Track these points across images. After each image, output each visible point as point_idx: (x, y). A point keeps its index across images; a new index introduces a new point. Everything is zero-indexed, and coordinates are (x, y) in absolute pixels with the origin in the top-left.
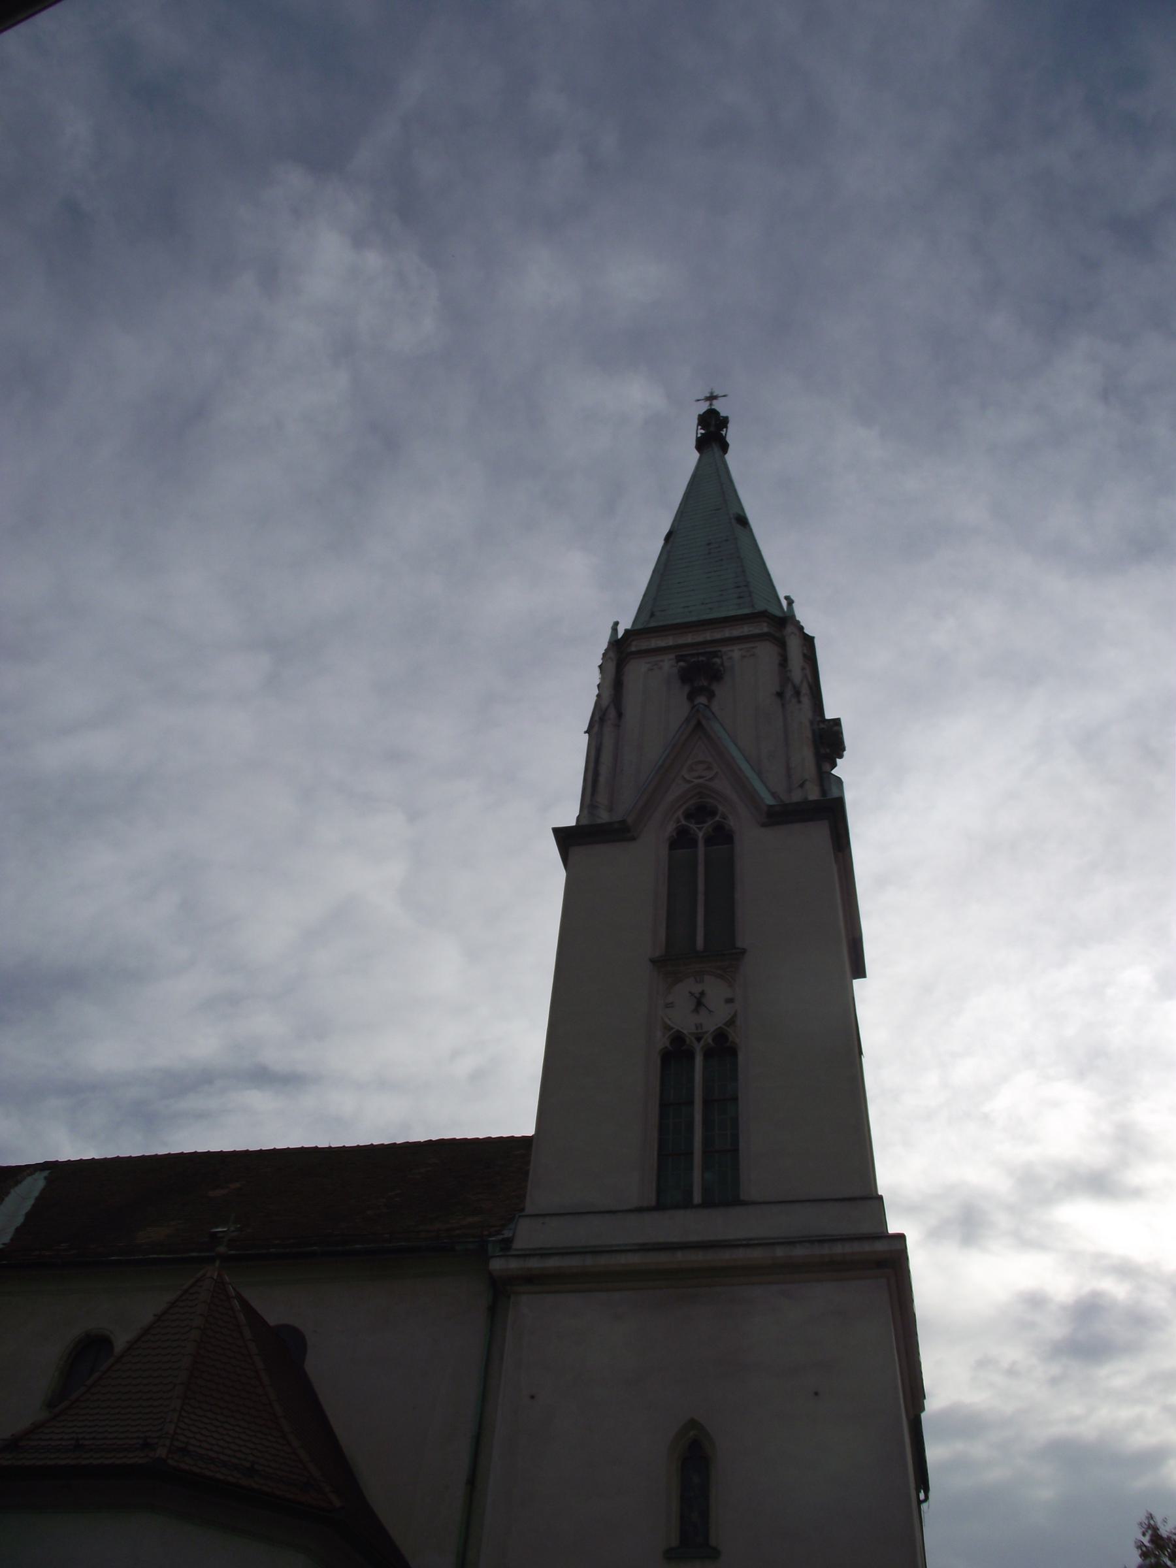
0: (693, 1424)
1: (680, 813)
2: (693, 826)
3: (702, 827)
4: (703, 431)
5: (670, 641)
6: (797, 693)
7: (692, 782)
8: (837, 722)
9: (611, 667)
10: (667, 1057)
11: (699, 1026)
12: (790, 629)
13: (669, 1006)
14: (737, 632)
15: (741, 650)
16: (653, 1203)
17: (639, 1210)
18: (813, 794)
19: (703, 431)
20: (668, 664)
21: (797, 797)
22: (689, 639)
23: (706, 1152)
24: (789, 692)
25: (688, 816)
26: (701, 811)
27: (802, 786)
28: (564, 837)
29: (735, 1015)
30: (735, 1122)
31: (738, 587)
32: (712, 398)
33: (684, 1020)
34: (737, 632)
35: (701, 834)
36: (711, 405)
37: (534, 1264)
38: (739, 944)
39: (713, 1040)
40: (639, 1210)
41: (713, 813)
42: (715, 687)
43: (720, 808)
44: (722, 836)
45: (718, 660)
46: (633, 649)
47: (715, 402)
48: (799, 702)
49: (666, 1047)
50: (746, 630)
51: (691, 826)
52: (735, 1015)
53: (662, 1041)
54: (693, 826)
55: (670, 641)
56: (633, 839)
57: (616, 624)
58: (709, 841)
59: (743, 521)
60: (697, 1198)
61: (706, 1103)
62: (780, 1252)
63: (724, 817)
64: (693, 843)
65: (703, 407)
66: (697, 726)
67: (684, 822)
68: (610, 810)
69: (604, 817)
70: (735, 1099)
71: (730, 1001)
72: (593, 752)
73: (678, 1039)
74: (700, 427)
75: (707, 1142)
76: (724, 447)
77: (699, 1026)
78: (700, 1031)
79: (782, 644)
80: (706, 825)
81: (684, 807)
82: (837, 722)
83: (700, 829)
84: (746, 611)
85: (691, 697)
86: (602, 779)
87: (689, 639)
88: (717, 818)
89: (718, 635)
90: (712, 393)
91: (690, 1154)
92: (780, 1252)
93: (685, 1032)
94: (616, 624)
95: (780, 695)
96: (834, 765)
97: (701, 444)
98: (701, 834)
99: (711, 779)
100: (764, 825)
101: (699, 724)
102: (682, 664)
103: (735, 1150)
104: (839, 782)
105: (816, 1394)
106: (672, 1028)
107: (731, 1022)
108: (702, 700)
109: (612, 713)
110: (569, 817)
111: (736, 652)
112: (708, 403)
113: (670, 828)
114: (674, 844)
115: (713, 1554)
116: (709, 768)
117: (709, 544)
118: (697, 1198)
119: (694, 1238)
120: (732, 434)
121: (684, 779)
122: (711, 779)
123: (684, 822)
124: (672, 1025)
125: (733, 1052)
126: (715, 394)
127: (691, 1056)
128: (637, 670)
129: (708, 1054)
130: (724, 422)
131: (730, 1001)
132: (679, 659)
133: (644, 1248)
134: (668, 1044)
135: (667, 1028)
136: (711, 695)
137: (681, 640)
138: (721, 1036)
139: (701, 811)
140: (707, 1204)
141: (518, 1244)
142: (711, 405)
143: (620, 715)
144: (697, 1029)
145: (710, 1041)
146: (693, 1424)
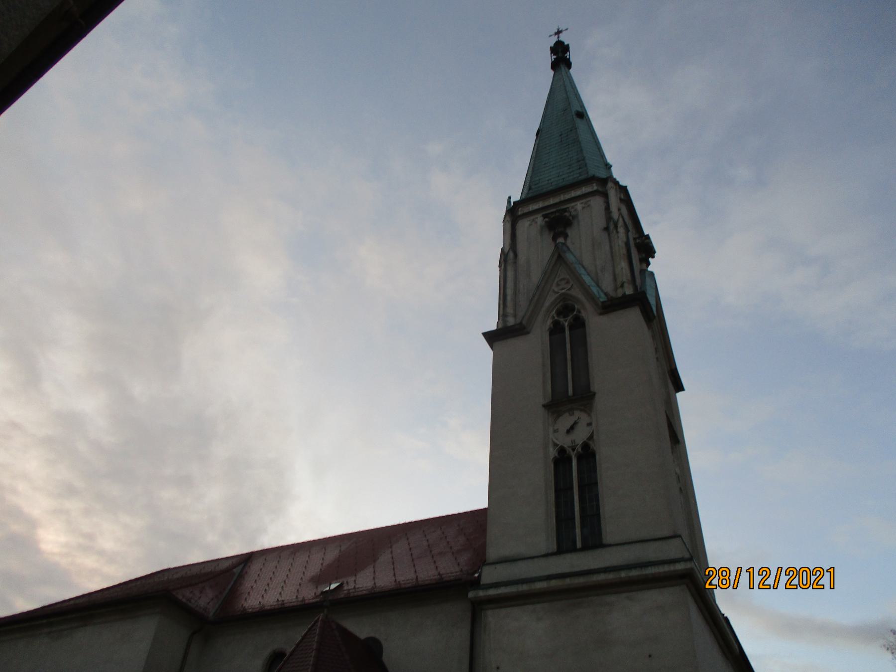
1: (554, 312)
2: (562, 320)
3: (567, 320)
4: (555, 57)
5: (540, 205)
6: (616, 227)
7: (559, 292)
8: (648, 235)
9: (509, 225)
10: (557, 462)
12: (610, 185)
13: (556, 431)
14: (578, 192)
15: (582, 203)
16: (554, 547)
17: (546, 555)
18: (629, 290)
19: (555, 57)
20: (540, 219)
21: (620, 293)
22: (552, 201)
24: (612, 227)
25: (559, 313)
27: (622, 286)
28: (491, 337)
29: (593, 432)
30: (597, 496)
32: (559, 32)
33: (565, 441)
34: (578, 192)
35: (566, 324)
36: (558, 37)
37: (492, 592)
38: (592, 389)
39: (582, 449)
40: (546, 555)
41: (573, 309)
42: (569, 232)
44: (579, 324)
45: (567, 214)
46: (520, 213)
47: (561, 35)
48: (617, 232)
49: (555, 457)
50: (585, 190)
52: (593, 432)
53: (552, 453)
54: (562, 320)
55: (540, 205)
56: (528, 333)
57: (510, 198)
59: (582, 115)
60: (579, 545)
61: (580, 487)
62: (623, 574)
63: (579, 312)
64: (562, 330)
65: (554, 39)
67: (556, 318)
68: (515, 316)
69: (511, 321)
70: (596, 483)
71: (589, 424)
72: (502, 282)
73: (562, 451)
74: (552, 55)
75: (582, 509)
76: (569, 65)
78: (574, 445)
79: (605, 195)
80: (569, 318)
82: (648, 235)
84: (583, 177)
85: (554, 239)
86: (509, 298)
87: (552, 201)
88: (575, 313)
89: (568, 196)
90: (558, 29)
91: (573, 518)
92: (623, 574)
93: (565, 446)
94: (510, 198)
95: (606, 229)
96: (648, 264)
97: (555, 66)
99: (569, 289)
100: (601, 314)
101: (560, 257)
102: (547, 219)
103: (598, 515)
104: (652, 274)
106: (559, 445)
107: (591, 437)
108: (561, 240)
109: (511, 255)
110: (492, 324)
111: (579, 205)
112: (557, 36)
113: (549, 322)
116: (568, 282)
117: (561, 135)
118: (579, 545)
119: (576, 569)
120: (574, 56)
121: (554, 291)
122: (569, 289)
123: (556, 318)
124: (558, 443)
126: (560, 30)
128: (524, 226)
129: (580, 458)
130: (566, 48)
131: (589, 424)
132: (545, 216)
133: (549, 578)
134: (557, 455)
135: (555, 445)
136: (566, 236)
137: (547, 203)
138: (586, 446)
140: (586, 548)
141: (485, 580)
142: (558, 37)
143: (516, 255)
144: (572, 444)
145: (580, 450)
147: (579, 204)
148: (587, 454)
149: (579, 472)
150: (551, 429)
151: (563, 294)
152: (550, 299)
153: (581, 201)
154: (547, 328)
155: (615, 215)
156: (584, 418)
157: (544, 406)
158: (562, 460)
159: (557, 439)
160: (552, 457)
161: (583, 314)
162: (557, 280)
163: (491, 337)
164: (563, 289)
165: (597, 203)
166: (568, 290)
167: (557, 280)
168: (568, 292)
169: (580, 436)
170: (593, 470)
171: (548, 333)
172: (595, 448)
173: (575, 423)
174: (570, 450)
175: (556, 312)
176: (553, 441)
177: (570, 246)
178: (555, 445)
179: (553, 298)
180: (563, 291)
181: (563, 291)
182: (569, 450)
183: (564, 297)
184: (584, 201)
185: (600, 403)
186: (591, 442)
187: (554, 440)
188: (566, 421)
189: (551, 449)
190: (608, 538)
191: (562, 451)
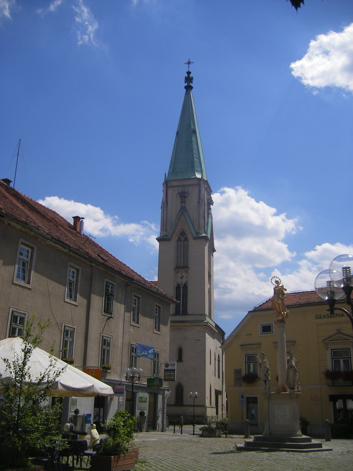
2: (181, 237)
10: (177, 287)
11: (182, 282)
23: (183, 306)
25: (180, 234)
26: (183, 233)
30: (187, 299)
33: (179, 281)
35: (183, 240)
44: (186, 239)
53: (176, 285)
54: (181, 237)
59: (194, 132)
66: (183, 210)
73: (178, 285)
77: (182, 282)
80: (183, 237)
86: (164, 223)
93: (180, 283)
107: (187, 282)
113: (177, 237)
114: (178, 241)
117: (186, 142)
128: (170, 191)
129: (183, 287)
131: (187, 277)
135: (177, 283)
138: (185, 284)
139: (183, 233)
143: (167, 204)
148: (185, 287)
149: (183, 291)
158: (178, 288)
164: (182, 226)
178: (177, 283)
180: (182, 227)
182: (180, 285)
190: (189, 312)
191: (178, 285)
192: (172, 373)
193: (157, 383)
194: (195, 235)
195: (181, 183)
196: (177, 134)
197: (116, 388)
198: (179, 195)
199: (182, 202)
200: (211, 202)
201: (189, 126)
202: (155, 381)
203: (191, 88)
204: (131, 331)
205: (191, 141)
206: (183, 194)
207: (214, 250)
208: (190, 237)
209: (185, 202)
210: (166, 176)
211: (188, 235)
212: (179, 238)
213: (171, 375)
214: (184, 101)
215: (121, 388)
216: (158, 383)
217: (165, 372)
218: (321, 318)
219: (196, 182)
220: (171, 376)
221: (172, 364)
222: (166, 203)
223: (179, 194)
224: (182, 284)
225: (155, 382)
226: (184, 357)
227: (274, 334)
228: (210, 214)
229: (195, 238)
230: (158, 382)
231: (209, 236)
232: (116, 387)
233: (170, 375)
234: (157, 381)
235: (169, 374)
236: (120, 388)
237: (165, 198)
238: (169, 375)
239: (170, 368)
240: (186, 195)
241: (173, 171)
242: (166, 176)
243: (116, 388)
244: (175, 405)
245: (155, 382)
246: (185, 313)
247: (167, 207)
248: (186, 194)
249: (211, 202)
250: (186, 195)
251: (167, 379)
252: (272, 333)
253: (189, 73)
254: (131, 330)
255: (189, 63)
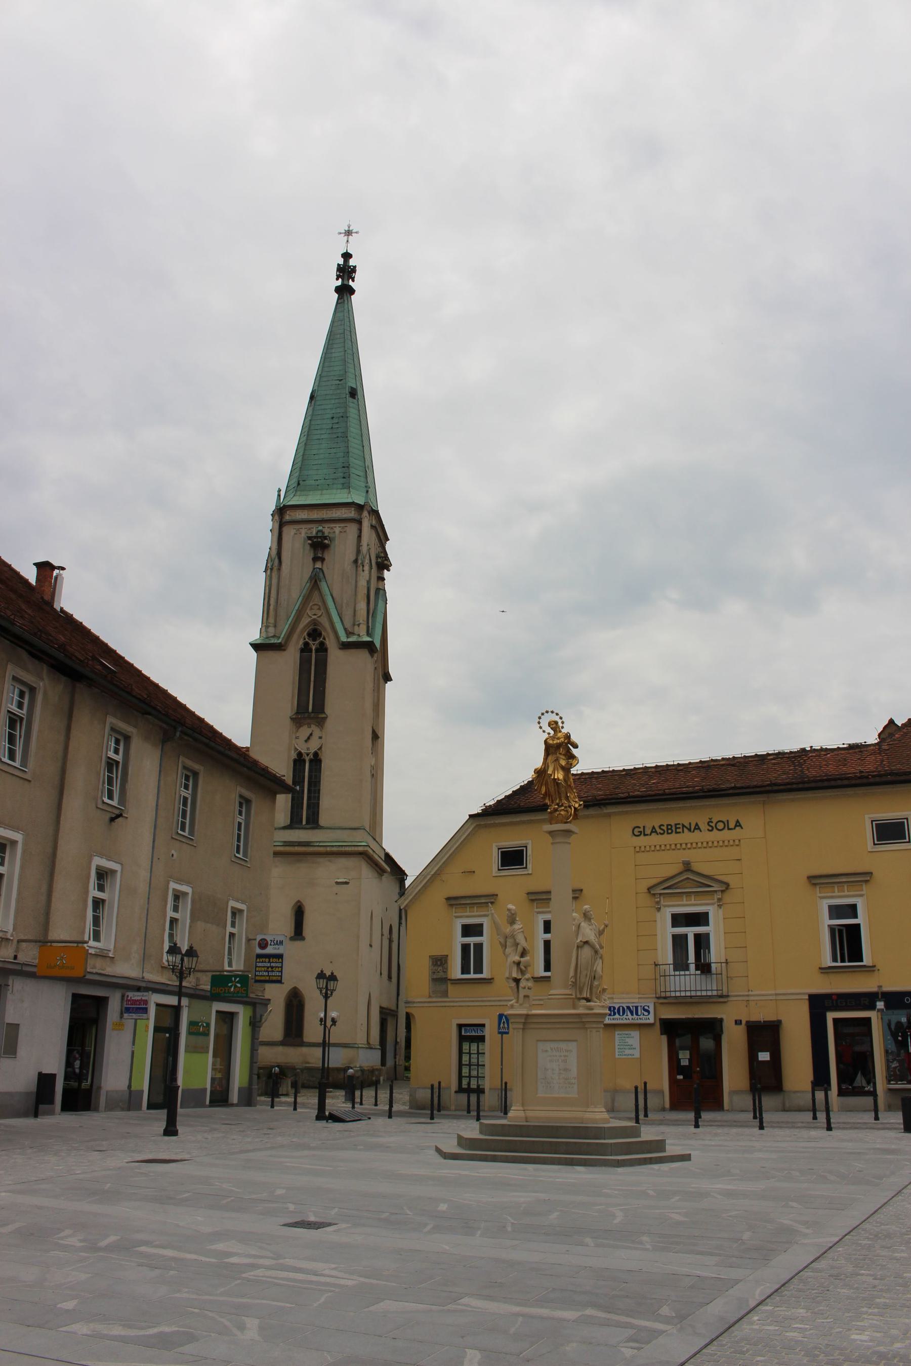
0: (299, 901)
1: (305, 634)
2: (311, 642)
10: (295, 761)
11: (308, 749)
13: (297, 738)
15: (339, 527)
25: (309, 635)
26: (315, 633)
28: (256, 647)
30: (319, 790)
31: (344, 467)
35: (314, 648)
39: (314, 756)
41: (320, 635)
43: (323, 633)
51: (310, 642)
52: (322, 746)
53: (294, 755)
54: (311, 642)
56: (284, 650)
58: (317, 650)
60: (304, 822)
63: (324, 639)
64: (311, 651)
67: (307, 640)
71: (320, 738)
73: (300, 754)
75: (309, 798)
79: (359, 522)
81: (308, 630)
83: (314, 644)
93: (302, 751)
95: (356, 561)
98: (314, 648)
105: (336, 894)
106: (298, 750)
107: (320, 748)
113: (301, 642)
114: (302, 651)
115: (303, 939)
116: (319, 609)
117: (333, 418)
118: (304, 822)
123: (307, 640)
125: (320, 761)
127: (304, 761)
128: (289, 532)
129: (311, 761)
131: (320, 738)
134: (296, 757)
135: (296, 749)
138: (316, 754)
139: (315, 633)
145: (312, 757)
146: (299, 901)
147: (338, 528)
148: (316, 760)
150: (294, 737)
151: (314, 619)
152: (305, 621)
153: (340, 525)
154: (299, 647)
155: (364, 549)
156: (317, 732)
157: (291, 718)
158: (299, 761)
159: (297, 744)
160: (293, 758)
161: (327, 642)
162: (311, 604)
163: (256, 647)
164: (315, 615)
165: (352, 529)
166: (318, 617)
167: (311, 604)
168: (318, 619)
169: (313, 746)
170: (319, 770)
171: (299, 651)
172: (322, 758)
173: (311, 734)
174: (306, 755)
175: (307, 633)
176: (295, 746)
177: (325, 569)
179: (307, 621)
180: (315, 617)
181: (315, 617)
183: (315, 622)
184: (342, 525)
185: (329, 724)
186: (319, 752)
187: (296, 745)
188: (305, 732)
189: (293, 752)
190: (322, 822)
191: (300, 754)
192: (276, 962)
193: (236, 986)
194: (344, 638)
195: (315, 515)
196: (312, 397)
197: (129, 998)
198: (310, 542)
199: (315, 559)
200: (386, 562)
201: (341, 380)
202: (232, 982)
203: (352, 291)
204: (173, 855)
205: (345, 417)
206: (319, 540)
207: (387, 678)
208: (331, 644)
209: (322, 560)
210: (279, 496)
211: (327, 639)
212: (306, 644)
213: (272, 967)
214: (333, 322)
215: (141, 1000)
216: (239, 987)
217: (258, 960)
218: (645, 835)
219: (351, 513)
220: (273, 971)
221: (275, 942)
222: (277, 561)
223: (309, 538)
224: (308, 755)
225: (230, 985)
226: (307, 930)
227: (530, 873)
228: (381, 592)
229: (346, 646)
230: (239, 985)
231: (378, 644)
232: (128, 996)
233: (270, 969)
234: (238, 982)
235: (269, 965)
236: (139, 998)
237: (275, 547)
238: (268, 967)
239: (270, 950)
240: (326, 541)
241: (299, 484)
242: (279, 496)
243: (129, 998)
244: (283, 1043)
245: (230, 985)
246: (314, 822)
247: (279, 569)
248: (326, 539)
249: (386, 562)
250: (326, 541)
251: (263, 978)
252: (526, 868)
253: (347, 256)
254: (173, 852)
255: (348, 233)
